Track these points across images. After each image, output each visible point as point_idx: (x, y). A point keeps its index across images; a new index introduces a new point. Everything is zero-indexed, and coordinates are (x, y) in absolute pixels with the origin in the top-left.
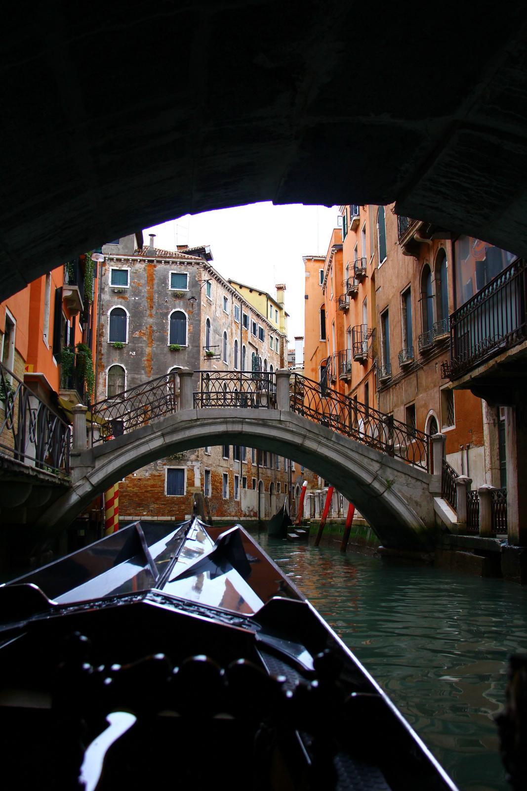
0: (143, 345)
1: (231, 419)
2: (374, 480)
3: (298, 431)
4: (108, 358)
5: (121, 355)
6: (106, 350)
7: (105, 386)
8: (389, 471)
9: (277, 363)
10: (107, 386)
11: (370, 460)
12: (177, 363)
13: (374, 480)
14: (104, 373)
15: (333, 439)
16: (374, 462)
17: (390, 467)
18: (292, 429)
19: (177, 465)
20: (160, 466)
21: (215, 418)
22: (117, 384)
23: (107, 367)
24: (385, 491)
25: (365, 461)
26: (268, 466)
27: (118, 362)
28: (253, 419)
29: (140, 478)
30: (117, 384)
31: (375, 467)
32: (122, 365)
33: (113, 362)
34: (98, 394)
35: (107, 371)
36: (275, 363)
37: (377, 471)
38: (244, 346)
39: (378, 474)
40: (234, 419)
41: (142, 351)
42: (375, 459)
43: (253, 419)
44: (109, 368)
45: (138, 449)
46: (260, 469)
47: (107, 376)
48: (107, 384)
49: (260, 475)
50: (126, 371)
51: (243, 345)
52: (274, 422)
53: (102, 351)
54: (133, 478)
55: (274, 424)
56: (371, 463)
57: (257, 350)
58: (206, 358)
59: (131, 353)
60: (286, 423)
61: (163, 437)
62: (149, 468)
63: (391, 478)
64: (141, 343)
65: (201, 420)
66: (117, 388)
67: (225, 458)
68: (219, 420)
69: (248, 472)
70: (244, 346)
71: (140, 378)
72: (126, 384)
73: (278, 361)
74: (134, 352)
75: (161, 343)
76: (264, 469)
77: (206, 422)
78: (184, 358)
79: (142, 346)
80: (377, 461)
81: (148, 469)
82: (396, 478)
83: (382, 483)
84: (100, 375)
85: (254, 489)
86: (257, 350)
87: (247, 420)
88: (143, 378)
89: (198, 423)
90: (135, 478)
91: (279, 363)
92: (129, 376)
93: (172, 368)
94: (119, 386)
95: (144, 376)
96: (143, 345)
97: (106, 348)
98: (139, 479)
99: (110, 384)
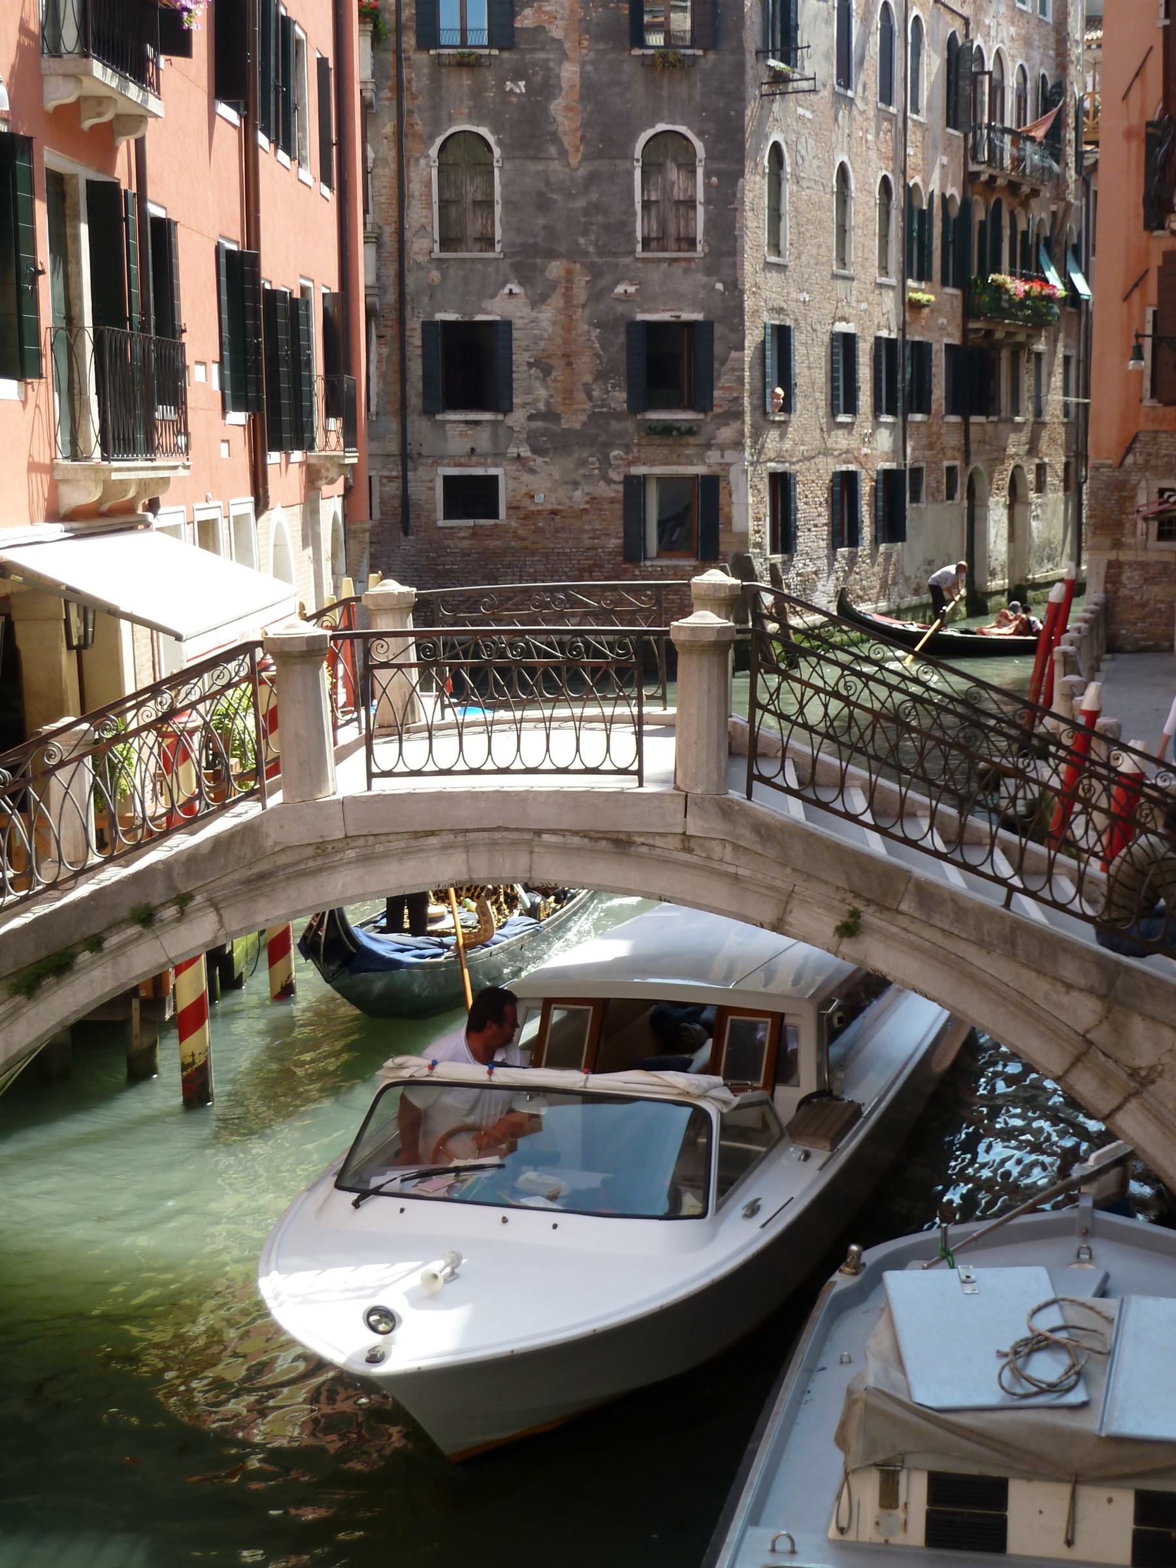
0: (552, 56)
1: (486, 834)
2: (1073, 1065)
3: (760, 876)
4: (435, 107)
5: (477, 93)
6: (425, 81)
7: (429, 205)
8: (1138, 1027)
9: (1044, 55)
10: (436, 207)
11: (1060, 988)
12: (666, 113)
13: (1073, 1065)
14: (422, 162)
15: (904, 907)
16: (1075, 994)
17: (1144, 1016)
18: (732, 869)
19: (675, 464)
20: (618, 466)
21: (416, 835)
22: (470, 196)
23: (432, 138)
24: (1119, 1108)
25: (1039, 989)
26: (1003, 414)
27: (470, 119)
28: (575, 833)
29: (556, 507)
30: (470, 196)
31: (1083, 1011)
32: (484, 131)
33: (451, 120)
34: (408, 235)
35: (433, 152)
36: (1036, 56)
37: (1087, 1031)
38: (917, 18)
39: (1090, 1043)
40: (497, 835)
41: (546, 79)
42: (1082, 982)
43: (575, 833)
44: (439, 141)
45: (123, 960)
46: (973, 429)
47: (435, 172)
48: (435, 198)
49: (973, 447)
50: (497, 152)
51: (914, 12)
52: (659, 842)
53: (414, 84)
54: (534, 508)
55: (658, 852)
56: (1065, 999)
57: (967, 22)
58: (765, 88)
59: (509, 85)
60: (708, 844)
61: (218, 910)
62: (584, 476)
63: (1145, 1058)
64: (543, 49)
65: (361, 842)
66: (470, 207)
67: (843, 418)
68: (433, 840)
69: (930, 447)
70: (917, 18)
71: (545, 171)
72: (497, 196)
73: (1046, 47)
74: (522, 84)
75: (611, 45)
76: (989, 428)
77: (379, 848)
78: (690, 98)
79: (546, 61)
80: (1091, 991)
81: (579, 479)
82: (1166, 1059)
83: (1105, 1080)
84: (412, 169)
85: (950, 496)
86: (967, 22)
87: (545, 837)
88: (554, 171)
89: (351, 854)
90: (540, 508)
91: (1052, 53)
92: (508, 166)
93: (650, 132)
94: (475, 203)
95: (556, 165)
96: (552, 56)
97: (426, 70)
98: (554, 513)
99: (447, 196)
